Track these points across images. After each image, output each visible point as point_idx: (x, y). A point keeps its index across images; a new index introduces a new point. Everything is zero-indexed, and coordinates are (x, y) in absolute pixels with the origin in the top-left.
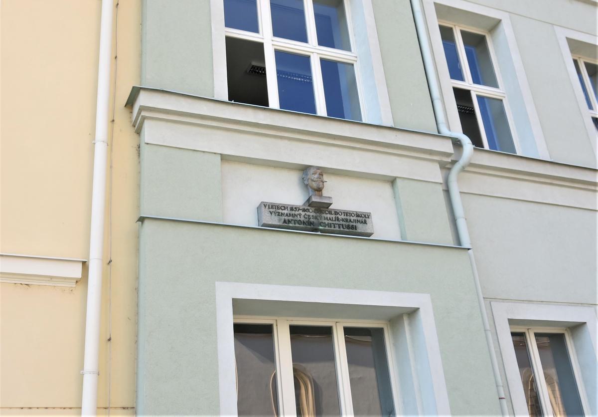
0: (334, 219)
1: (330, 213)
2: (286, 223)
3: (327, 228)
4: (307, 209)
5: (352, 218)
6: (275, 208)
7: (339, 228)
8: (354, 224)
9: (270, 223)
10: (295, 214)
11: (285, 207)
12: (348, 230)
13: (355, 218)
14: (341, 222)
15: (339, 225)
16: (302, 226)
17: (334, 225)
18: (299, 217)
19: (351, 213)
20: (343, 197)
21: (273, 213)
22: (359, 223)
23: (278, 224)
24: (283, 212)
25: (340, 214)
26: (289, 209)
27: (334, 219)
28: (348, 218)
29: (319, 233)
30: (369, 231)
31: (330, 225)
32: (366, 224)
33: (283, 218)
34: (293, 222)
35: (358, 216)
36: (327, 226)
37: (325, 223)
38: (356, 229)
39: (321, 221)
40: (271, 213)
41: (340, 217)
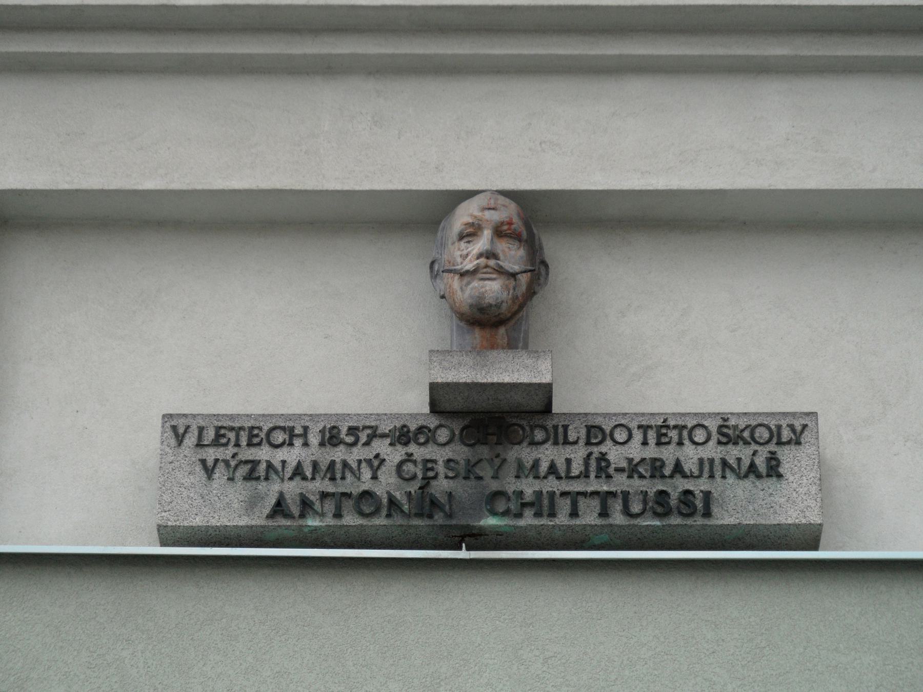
0: (576, 469)
1: (560, 437)
2: (288, 516)
3: (528, 520)
4: (421, 429)
5: (690, 455)
6: (223, 444)
7: (604, 514)
8: (699, 486)
10: (345, 464)
11: (290, 432)
12: (658, 523)
13: (712, 451)
14: (620, 483)
15: (605, 497)
18: (366, 474)
19: (690, 423)
20: (651, 350)
21: (220, 473)
22: (731, 479)
23: (244, 521)
24: (282, 454)
25: (620, 436)
26: (314, 440)
27: (576, 469)
28: (668, 454)
29: (463, 554)
31: (543, 505)
32: (780, 476)
33: (272, 490)
34: (329, 506)
35: (728, 434)
36: (528, 513)
37: (520, 494)
38: (707, 514)
39: (494, 486)
40: (209, 471)
41: (616, 455)
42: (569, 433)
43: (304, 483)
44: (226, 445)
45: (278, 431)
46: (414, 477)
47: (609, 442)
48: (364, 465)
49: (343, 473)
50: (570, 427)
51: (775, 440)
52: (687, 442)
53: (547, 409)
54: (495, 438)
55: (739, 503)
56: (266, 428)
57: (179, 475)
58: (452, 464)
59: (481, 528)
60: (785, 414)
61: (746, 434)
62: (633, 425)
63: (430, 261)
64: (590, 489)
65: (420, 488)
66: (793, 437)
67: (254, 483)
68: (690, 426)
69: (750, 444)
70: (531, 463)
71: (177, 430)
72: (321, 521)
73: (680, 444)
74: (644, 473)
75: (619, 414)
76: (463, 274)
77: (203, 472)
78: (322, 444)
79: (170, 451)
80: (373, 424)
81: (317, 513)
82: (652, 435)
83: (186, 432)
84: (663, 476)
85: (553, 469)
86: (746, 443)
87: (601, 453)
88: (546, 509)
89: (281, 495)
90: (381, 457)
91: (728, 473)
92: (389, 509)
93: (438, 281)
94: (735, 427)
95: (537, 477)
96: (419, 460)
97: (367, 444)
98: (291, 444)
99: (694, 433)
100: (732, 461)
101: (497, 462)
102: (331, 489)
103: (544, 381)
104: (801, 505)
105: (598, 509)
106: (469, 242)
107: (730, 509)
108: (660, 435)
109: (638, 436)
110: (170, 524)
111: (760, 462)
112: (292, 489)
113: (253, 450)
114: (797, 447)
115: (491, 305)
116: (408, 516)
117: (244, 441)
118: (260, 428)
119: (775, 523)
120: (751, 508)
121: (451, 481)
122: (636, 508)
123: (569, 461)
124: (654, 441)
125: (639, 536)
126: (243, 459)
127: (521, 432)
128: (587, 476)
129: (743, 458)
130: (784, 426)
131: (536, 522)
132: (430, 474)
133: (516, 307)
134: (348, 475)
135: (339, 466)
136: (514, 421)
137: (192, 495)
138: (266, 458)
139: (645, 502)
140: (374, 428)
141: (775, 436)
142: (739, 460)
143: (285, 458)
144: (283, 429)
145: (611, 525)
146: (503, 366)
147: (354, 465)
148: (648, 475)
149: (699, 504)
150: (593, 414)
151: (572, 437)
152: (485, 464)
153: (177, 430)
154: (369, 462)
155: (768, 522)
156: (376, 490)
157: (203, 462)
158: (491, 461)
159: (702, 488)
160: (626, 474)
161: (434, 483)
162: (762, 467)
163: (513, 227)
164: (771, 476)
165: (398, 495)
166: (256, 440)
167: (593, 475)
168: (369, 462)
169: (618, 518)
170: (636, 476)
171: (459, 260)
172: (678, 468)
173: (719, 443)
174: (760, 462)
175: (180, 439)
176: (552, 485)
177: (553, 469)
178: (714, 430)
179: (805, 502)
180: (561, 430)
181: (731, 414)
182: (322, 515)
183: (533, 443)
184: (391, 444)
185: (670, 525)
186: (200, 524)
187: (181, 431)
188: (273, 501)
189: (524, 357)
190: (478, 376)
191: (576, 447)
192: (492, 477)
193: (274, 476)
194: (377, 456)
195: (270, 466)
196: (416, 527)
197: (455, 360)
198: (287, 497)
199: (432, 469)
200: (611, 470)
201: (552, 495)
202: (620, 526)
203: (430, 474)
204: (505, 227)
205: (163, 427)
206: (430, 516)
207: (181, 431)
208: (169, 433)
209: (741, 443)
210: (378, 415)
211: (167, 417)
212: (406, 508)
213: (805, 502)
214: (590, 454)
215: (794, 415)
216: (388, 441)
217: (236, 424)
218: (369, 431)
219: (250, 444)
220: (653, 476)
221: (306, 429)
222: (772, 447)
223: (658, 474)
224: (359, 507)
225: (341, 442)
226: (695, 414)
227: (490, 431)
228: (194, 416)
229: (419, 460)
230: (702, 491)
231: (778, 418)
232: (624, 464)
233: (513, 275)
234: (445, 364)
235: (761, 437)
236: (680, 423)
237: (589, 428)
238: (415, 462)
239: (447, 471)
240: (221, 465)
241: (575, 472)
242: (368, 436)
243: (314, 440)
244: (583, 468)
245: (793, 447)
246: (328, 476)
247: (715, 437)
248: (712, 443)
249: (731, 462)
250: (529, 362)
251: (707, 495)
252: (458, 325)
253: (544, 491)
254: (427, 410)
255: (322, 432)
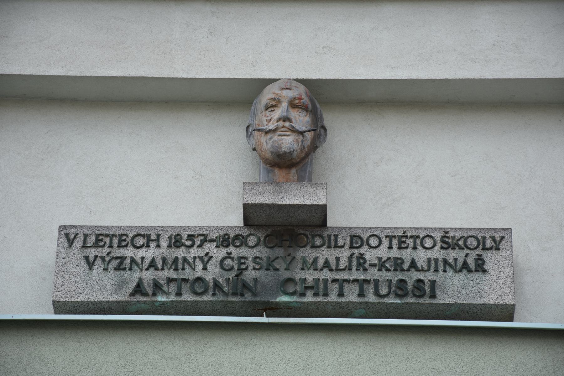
0: (343, 264)
1: (332, 243)
2: (145, 294)
3: (309, 298)
4: (237, 237)
5: (421, 256)
6: (100, 246)
7: (361, 294)
8: (427, 277)
9: (81, 298)
10: (185, 260)
11: (148, 238)
12: (398, 301)
13: (437, 253)
14: (373, 274)
16: (208, 298)
17: (341, 289)
18: (199, 266)
21: (98, 264)
22: (450, 273)
24: (141, 253)
25: (374, 242)
26: (164, 243)
27: (343, 264)
28: (407, 255)
29: (264, 319)
30: (492, 298)
32: (484, 271)
33: (135, 276)
34: (173, 287)
36: (309, 293)
38: (433, 296)
39: (287, 275)
40: (90, 264)
41: (370, 255)
42: (339, 240)
43: (157, 272)
44: (103, 246)
45: (140, 237)
46: (232, 268)
47: (365, 247)
48: (197, 260)
49: (183, 265)
50: (339, 236)
51: (481, 247)
52: (419, 247)
53: (324, 223)
54: (288, 243)
55: (455, 289)
56: (131, 235)
57: (69, 266)
58: (258, 260)
59: (277, 303)
60: (488, 229)
61: (461, 242)
62: (383, 235)
63: (247, 125)
64: (352, 278)
65: (236, 276)
66: (494, 245)
67: (122, 272)
68: (421, 236)
69: (464, 249)
70: (312, 259)
71: (69, 236)
72: (167, 298)
73: (415, 248)
74: (389, 267)
75: (373, 228)
76: (267, 132)
77: (86, 265)
78: (169, 246)
79: (64, 251)
80: (205, 233)
81: (164, 292)
82: (395, 242)
83: (75, 237)
84: (403, 270)
85: (327, 264)
86: (461, 248)
87: (360, 254)
88: (321, 292)
89: (140, 280)
90: (210, 255)
91: (448, 268)
92: (214, 290)
93: (251, 139)
94: (453, 238)
95: (316, 269)
96: (236, 257)
97: (200, 246)
98: (148, 246)
99: (424, 241)
100: (451, 261)
101: (289, 259)
102: (174, 275)
103: (321, 203)
104: (499, 291)
105: (357, 292)
106: (272, 111)
107: (449, 293)
108: (401, 242)
109: (386, 243)
110: (62, 300)
111: (471, 261)
112: (148, 276)
113: (122, 250)
114: (497, 252)
115: (286, 153)
116: (226, 294)
117: (115, 244)
118: (127, 235)
119: (481, 303)
120: (464, 292)
121: (257, 272)
122: (383, 291)
123: (338, 259)
124: (397, 246)
125: (386, 311)
126: (115, 256)
127: (306, 239)
128: (350, 269)
129: (459, 258)
130: (488, 237)
131: (315, 299)
132: (243, 266)
133: (303, 155)
134: (187, 267)
135: (180, 261)
136: (302, 231)
137: (78, 280)
138: (130, 255)
139: (390, 287)
140: (205, 236)
141: (481, 244)
142: (456, 260)
143: (144, 255)
144: (143, 236)
145: (366, 303)
146: (293, 193)
147: (191, 260)
148: (392, 269)
149: (427, 288)
150: (355, 228)
151: (340, 242)
152: (280, 260)
153: (69, 236)
154: (201, 258)
155: (476, 302)
156: (206, 277)
157: (87, 258)
158: (284, 259)
159: (430, 278)
160: (377, 268)
161: (245, 273)
162: (472, 265)
163: (302, 101)
164: (478, 271)
165: (220, 280)
166: (124, 243)
167: (354, 268)
168: (201, 258)
169: (371, 298)
170: (384, 269)
171: (265, 123)
172: (413, 265)
173: (442, 248)
174: (471, 261)
175: (71, 242)
176: (326, 274)
177: (327, 264)
178: (438, 239)
179: (503, 290)
180: (333, 238)
181: (451, 228)
182: (168, 294)
183: (314, 247)
184: (217, 247)
185: (407, 303)
186: (83, 300)
187: (72, 237)
188: (135, 284)
189: (308, 187)
190: (277, 199)
191: (343, 249)
192: (285, 269)
193: (136, 268)
194: (207, 254)
195: (133, 260)
196: (233, 302)
197: (260, 189)
198: (144, 281)
199: (244, 263)
200: (367, 265)
201: (326, 281)
202: (373, 303)
203: (243, 266)
204: (297, 101)
205: (59, 234)
206: (242, 295)
207: (72, 237)
208: (64, 238)
209: (457, 248)
210: (208, 227)
211: (62, 228)
212: (226, 289)
213: (503, 290)
214: (353, 254)
215: (495, 230)
216: (215, 244)
217: (111, 233)
218: (202, 238)
219: (119, 246)
220: (395, 270)
221: (158, 236)
222: (479, 251)
223: (398, 268)
224: (193, 288)
225: (182, 245)
226: (426, 229)
227: (284, 238)
228: (81, 227)
229: (236, 257)
230: (429, 280)
231: (483, 232)
232: (376, 262)
233: (302, 133)
234: (254, 191)
235: (471, 245)
236: (415, 234)
237: (352, 237)
238: (232, 259)
239: (254, 265)
240: (99, 261)
241: (342, 266)
242: (201, 241)
243: (164, 243)
244: (347, 264)
245: (494, 252)
246: (173, 267)
247: (439, 244)
248: (437, 248)
249: (450, 261)
250: (311, 190)
251: (433, 283)
252: (264, 168)
253: (321, 279)
254: (242, 224)
255: (170, 238)
